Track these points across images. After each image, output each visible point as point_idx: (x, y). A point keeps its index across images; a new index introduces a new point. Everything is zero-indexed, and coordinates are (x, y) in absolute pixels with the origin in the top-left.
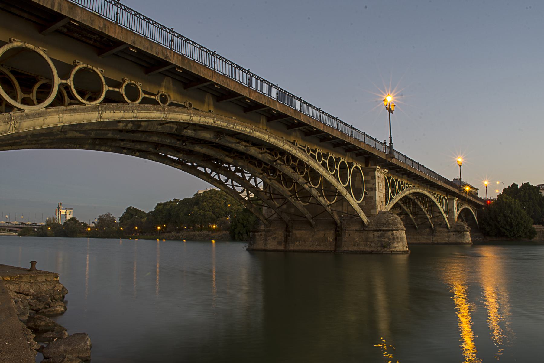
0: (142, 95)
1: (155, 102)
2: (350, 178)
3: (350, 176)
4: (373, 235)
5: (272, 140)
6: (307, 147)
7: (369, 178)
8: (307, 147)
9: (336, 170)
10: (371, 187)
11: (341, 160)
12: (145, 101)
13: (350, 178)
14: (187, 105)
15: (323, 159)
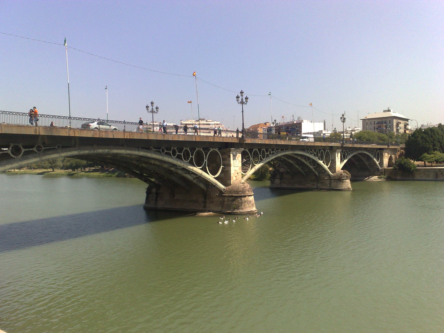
0: (23, 150)
1: (33, 152)
2: (206, 160)
3: (206, 159)
4: (228, 199)
5: (129, 152)
6: (161, 149)
7: (224, 156)
8: (161, 149)
9: (192, 158)
10: (228, 163)
11: (197, 149)
12: (26, 153)
13: (206, 160)
14: (56, 147)
15: (177, 153)
